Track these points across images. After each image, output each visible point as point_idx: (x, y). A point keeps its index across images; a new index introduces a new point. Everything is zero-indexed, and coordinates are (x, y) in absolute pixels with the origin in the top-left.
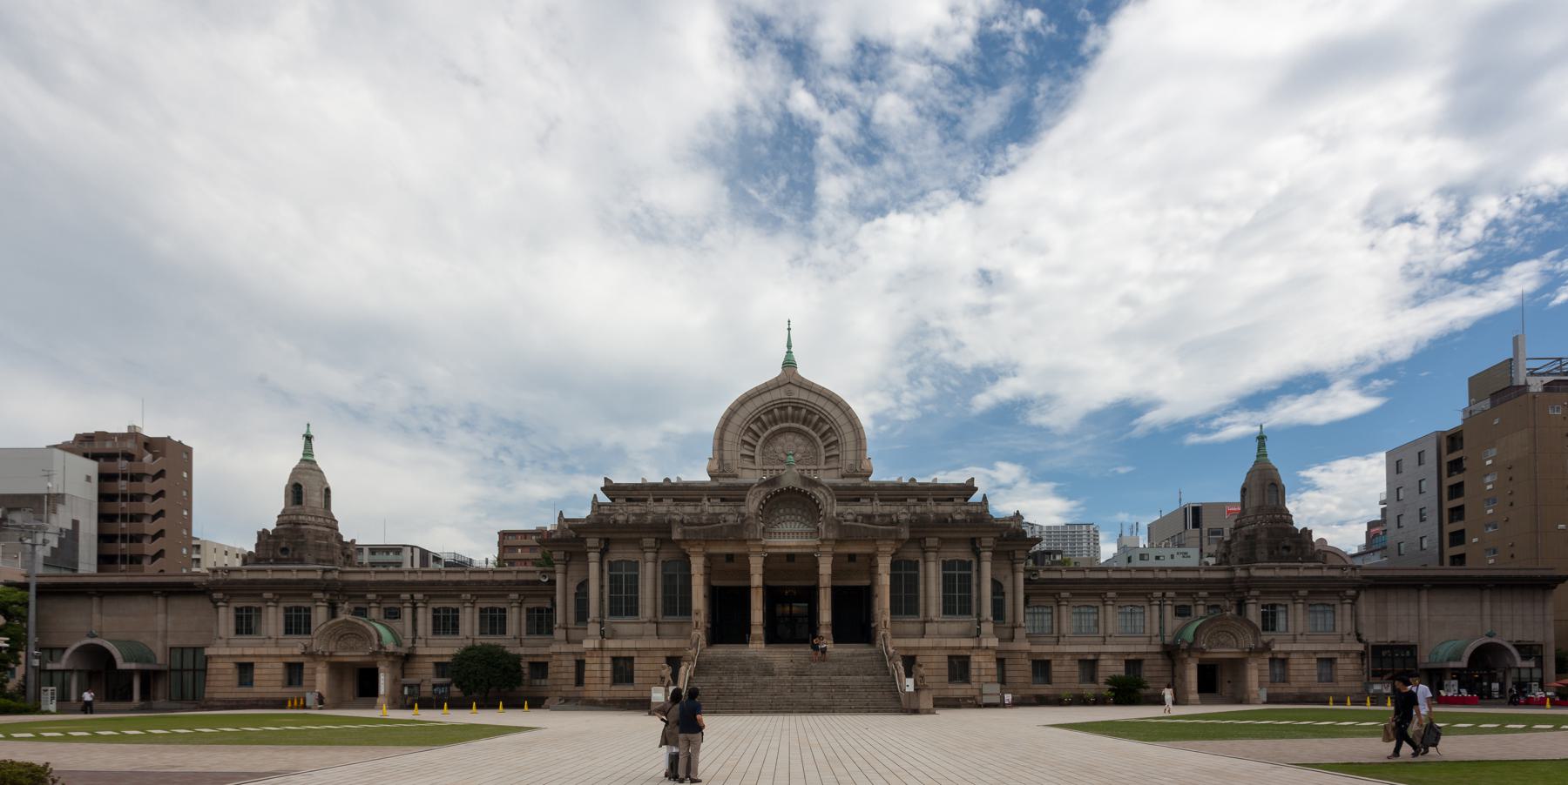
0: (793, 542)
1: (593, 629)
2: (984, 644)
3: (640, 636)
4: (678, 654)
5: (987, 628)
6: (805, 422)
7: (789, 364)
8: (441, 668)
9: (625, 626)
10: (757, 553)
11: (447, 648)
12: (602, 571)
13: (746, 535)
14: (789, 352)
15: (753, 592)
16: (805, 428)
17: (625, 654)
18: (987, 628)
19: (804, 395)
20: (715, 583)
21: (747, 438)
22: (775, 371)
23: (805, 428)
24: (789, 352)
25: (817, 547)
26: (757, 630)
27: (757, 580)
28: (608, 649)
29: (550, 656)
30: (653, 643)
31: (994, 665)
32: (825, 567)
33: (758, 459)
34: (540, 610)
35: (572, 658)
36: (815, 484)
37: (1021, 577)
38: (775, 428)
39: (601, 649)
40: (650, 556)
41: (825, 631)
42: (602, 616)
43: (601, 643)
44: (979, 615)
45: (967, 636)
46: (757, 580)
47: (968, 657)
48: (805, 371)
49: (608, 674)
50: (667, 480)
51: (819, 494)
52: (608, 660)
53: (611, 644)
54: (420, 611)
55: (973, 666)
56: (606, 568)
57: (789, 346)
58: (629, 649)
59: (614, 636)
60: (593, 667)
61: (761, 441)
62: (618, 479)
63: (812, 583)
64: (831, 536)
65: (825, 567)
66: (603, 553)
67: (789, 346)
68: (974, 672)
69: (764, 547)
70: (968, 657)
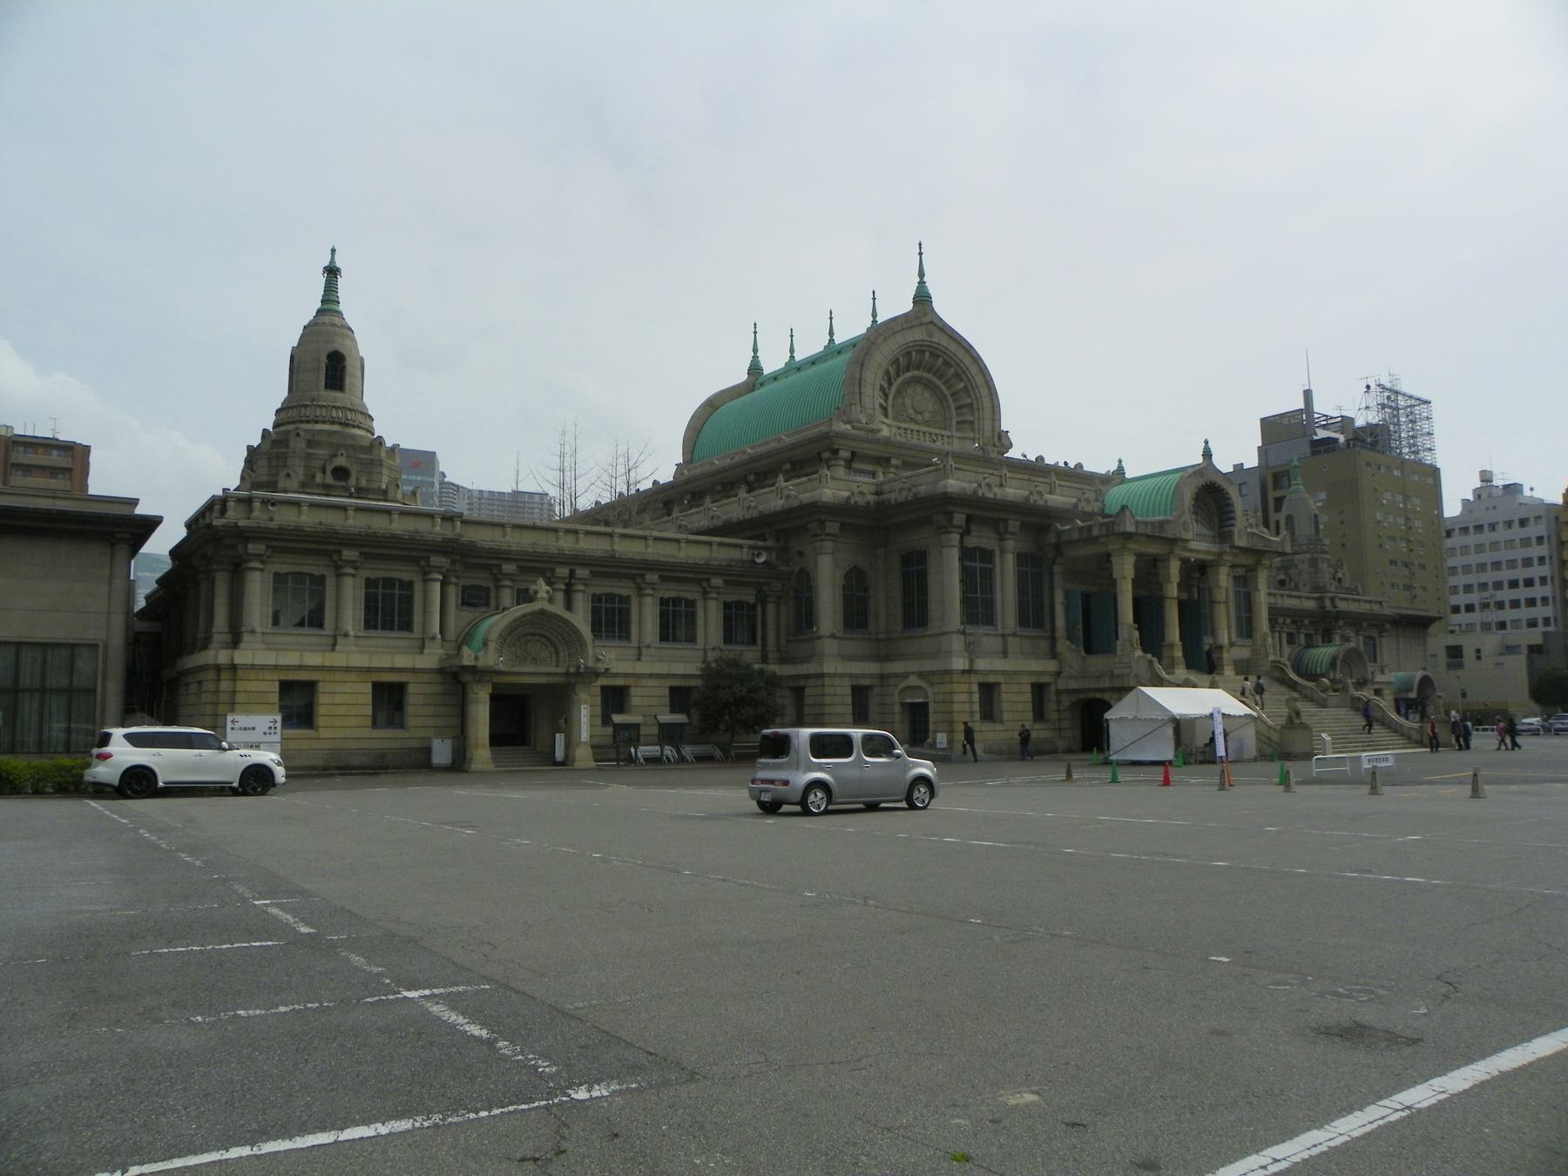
8: (679, 697)
9: (987, 639)
11: (684, 663)
19: (945, 341)
24: (922, 283)
28: (976, 672)
33: (890, 410)
34: (740, 605)
35: (847, 682)
39: (969, 672)
43: (971, 662)
46: (1172, 590)
49: (977, 707)
52: (975, 688)
57: (921, 274)
60: (964, 697)
67: (921, 274)
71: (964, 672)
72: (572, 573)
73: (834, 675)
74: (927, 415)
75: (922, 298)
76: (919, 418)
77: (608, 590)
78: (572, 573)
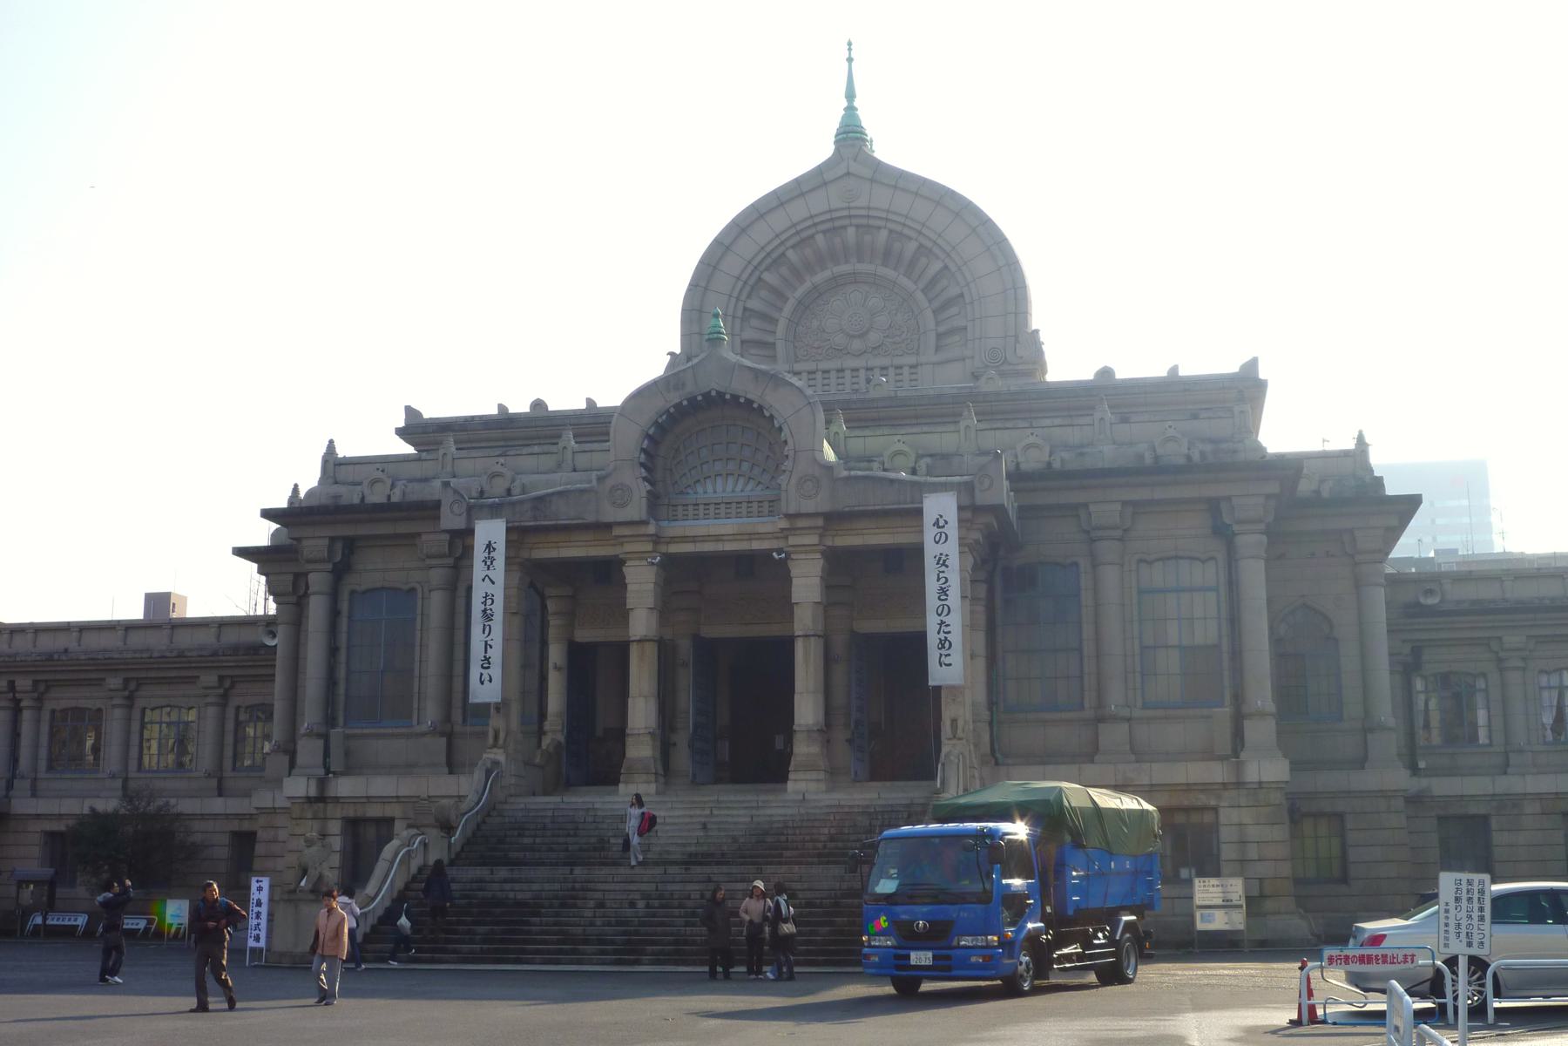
0: (727, 526)
1: (309, 751)
2: (1252, 773)
3: (407, 768)
4: (246, 826)
5: (1260, 732)
6: (887, 256)
7: (851, 136)
10: (641, 556)
12: (334, 613)
13: (610, 514)
14: (850, 110)
15: (634, 652)
16: (889, 273)
17: (374, 811)
18: (1260, 732)
20: (583, 635)
21: (754, 304)
22: (814, 149)
23: (889, 273)
24: (850, 110)
25: (785, 533)
26: (640, 750)
27: (641, 623)
28: (337, 800)
29: (251, 817)
30: (442, 786)
31: (1280, 832)
32: (806, 584)
33: (780, 346)
36: (775, 380)
37: (1378, 599)
38: (820, 277)
39: (321, 799)
40: (437, 576)
41: (803, 749)
42: (330, 720)
43: (322, 783)
44: (1238, 698)
45: (1209, 755)
46: (641, 623)
47: (1215, 809)
48: (893, 147)
50: (538, 405)
51: (778, 403)
52: (335, 827)
53: (344, 787)
54: (27, 715)
55: (1226, 834)
56: (344, 606)
57: (850, 95)
58: (384, 800)
59: (348, 771)
61: (788, 308)
62: (434, 409)
63: (775, 630)
64: (809, 506)
65: (806, 584)
66: (340, 572)
67: (850, 95)
68: (1228, 852)
69: (657, 539)
70: (1215, 809)
71: (309, 800)
72: (12, 685)
73: (274, 811)
74: (874, 337)
75: (851, 136)
76: (857, 345)
77: (73, 704)
78: (12, 685)
